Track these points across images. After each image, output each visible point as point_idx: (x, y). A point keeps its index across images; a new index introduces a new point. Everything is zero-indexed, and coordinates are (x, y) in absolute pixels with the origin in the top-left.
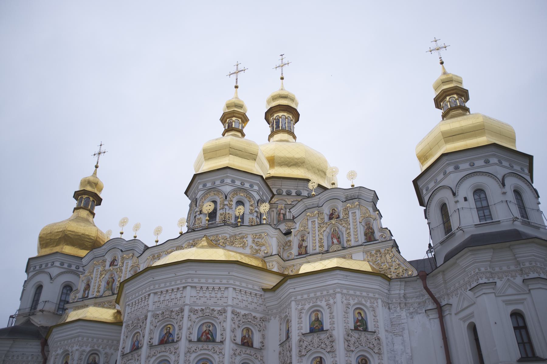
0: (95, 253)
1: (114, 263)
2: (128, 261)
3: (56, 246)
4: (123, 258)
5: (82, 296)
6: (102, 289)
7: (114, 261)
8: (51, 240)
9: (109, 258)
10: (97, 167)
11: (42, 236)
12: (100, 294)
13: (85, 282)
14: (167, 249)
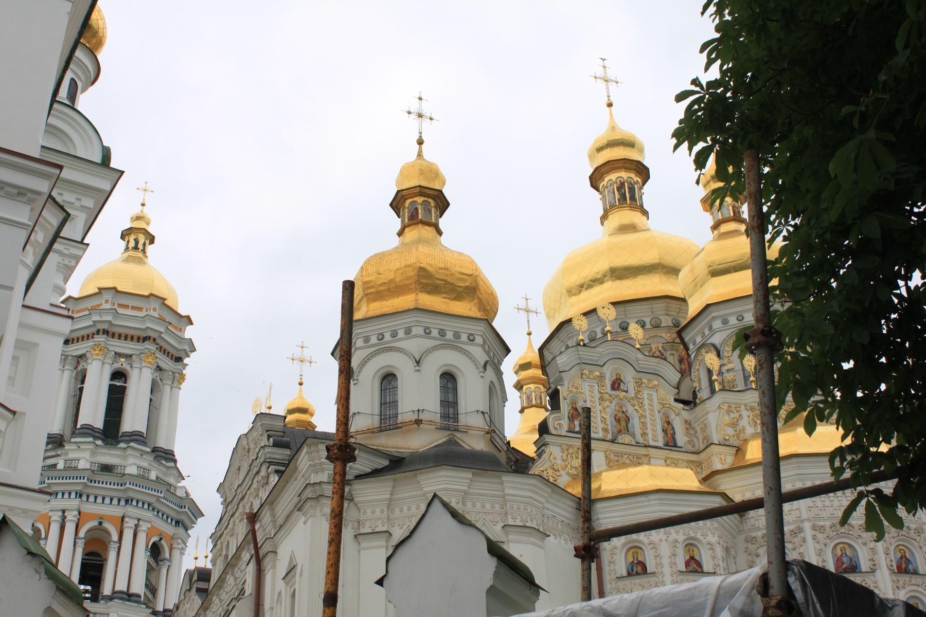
0: (580, 353)
1: (619, 386)
2: (651, 393)
3: (455, 299)
4: (639, 383)
5: (569, 427)
6: (609, 428)
7: (618, 381)
8: (445, 284)
9: (609, 374)
10: (420, 142)
11: (426, 267)
12: (610, 437)
13: (568, 401)
14: (747, 402)
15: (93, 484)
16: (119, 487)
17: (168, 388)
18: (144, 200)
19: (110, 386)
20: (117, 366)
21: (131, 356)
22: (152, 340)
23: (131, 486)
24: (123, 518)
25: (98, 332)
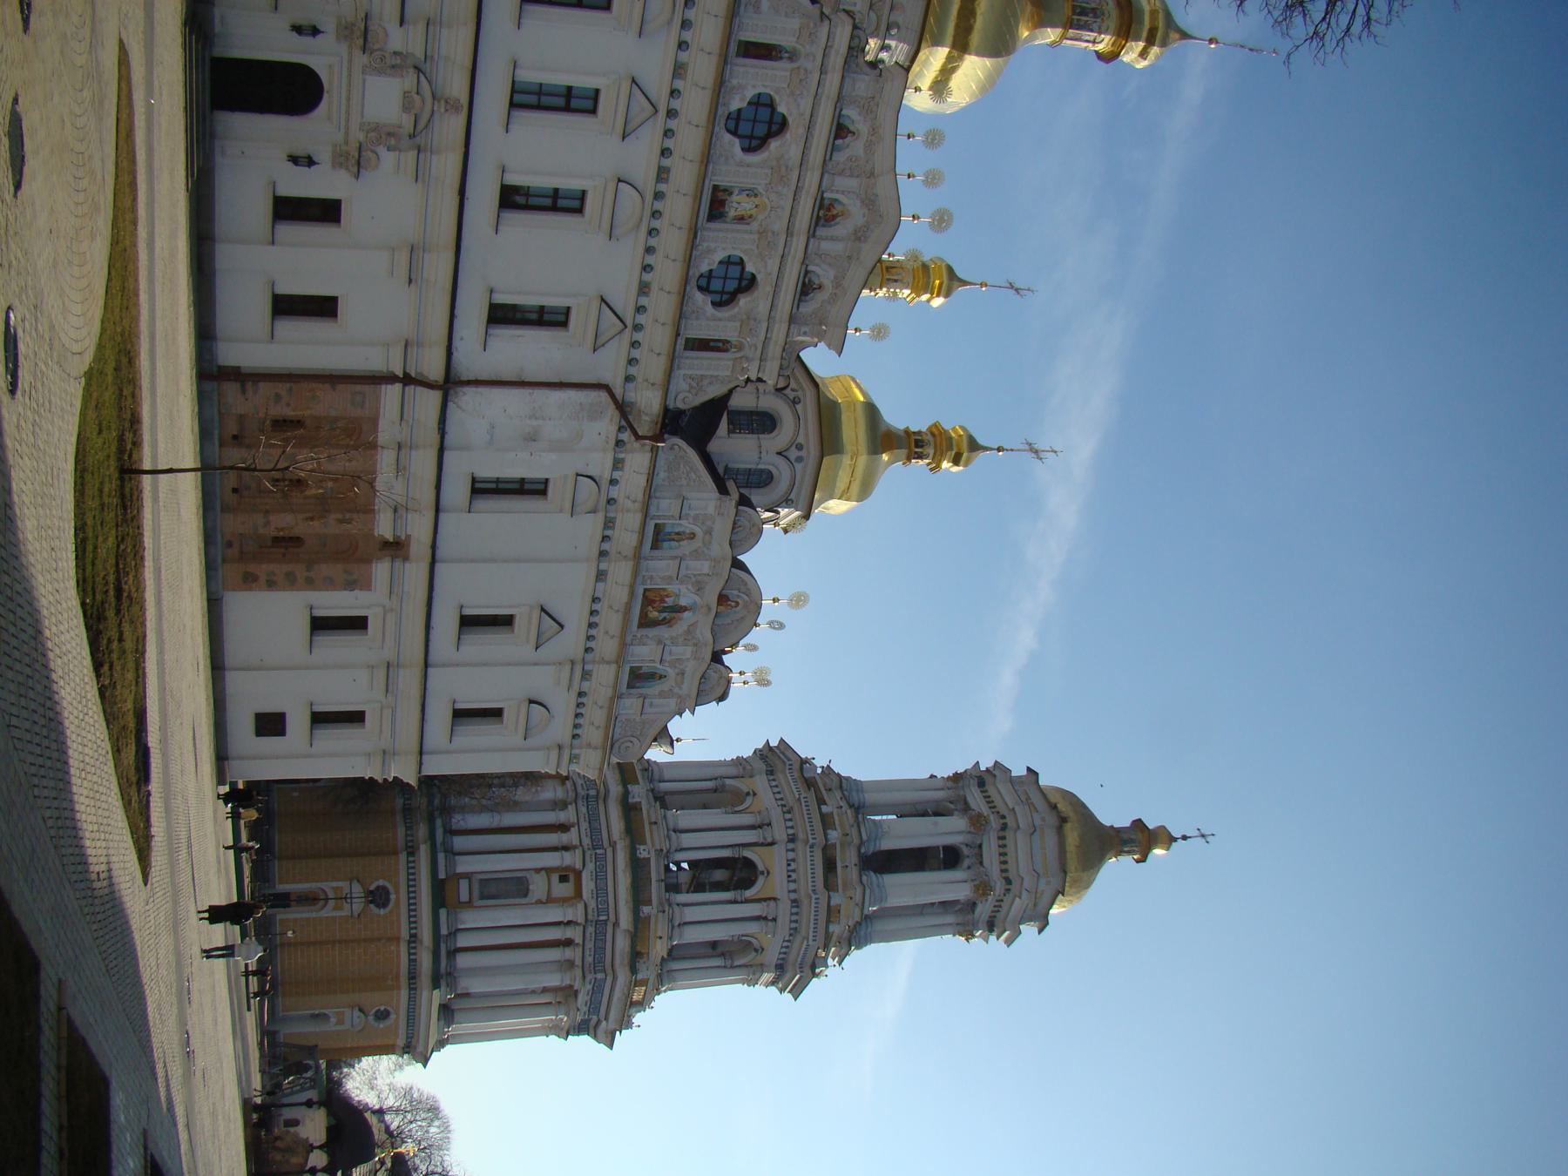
15: (808, 850)
16: (810, 888)
17: (950, 919)
18: (1190, 837)
19: (938, 847)
20: (966, 851)
21: (981, 863)
22: (1008, 887)
23: (813, 901)
24: (775, 899)
25: (1003, 817)
